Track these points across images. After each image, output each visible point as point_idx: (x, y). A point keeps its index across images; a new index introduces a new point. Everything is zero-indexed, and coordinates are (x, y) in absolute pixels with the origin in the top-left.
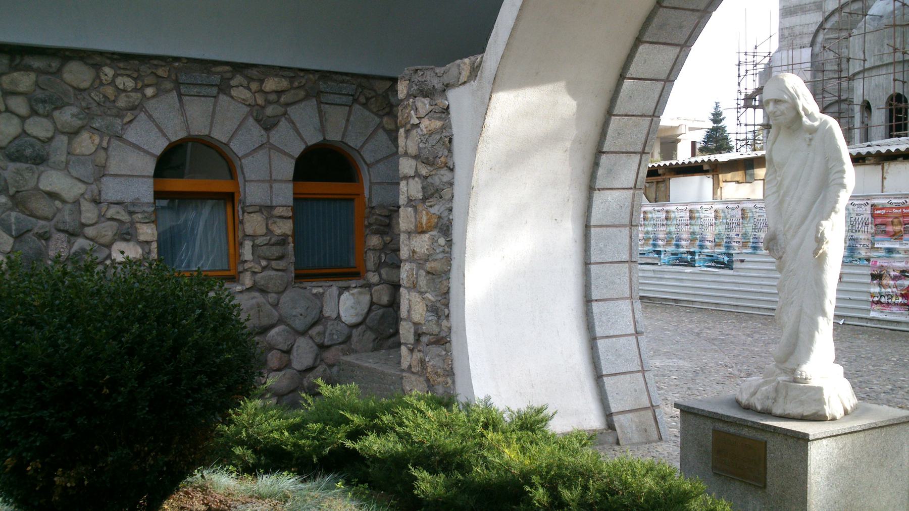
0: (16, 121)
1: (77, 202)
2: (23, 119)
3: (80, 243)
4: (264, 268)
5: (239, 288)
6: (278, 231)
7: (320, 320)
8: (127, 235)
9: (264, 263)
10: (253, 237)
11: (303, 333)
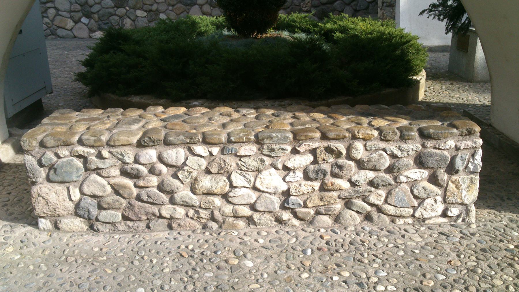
11: (349, 4)
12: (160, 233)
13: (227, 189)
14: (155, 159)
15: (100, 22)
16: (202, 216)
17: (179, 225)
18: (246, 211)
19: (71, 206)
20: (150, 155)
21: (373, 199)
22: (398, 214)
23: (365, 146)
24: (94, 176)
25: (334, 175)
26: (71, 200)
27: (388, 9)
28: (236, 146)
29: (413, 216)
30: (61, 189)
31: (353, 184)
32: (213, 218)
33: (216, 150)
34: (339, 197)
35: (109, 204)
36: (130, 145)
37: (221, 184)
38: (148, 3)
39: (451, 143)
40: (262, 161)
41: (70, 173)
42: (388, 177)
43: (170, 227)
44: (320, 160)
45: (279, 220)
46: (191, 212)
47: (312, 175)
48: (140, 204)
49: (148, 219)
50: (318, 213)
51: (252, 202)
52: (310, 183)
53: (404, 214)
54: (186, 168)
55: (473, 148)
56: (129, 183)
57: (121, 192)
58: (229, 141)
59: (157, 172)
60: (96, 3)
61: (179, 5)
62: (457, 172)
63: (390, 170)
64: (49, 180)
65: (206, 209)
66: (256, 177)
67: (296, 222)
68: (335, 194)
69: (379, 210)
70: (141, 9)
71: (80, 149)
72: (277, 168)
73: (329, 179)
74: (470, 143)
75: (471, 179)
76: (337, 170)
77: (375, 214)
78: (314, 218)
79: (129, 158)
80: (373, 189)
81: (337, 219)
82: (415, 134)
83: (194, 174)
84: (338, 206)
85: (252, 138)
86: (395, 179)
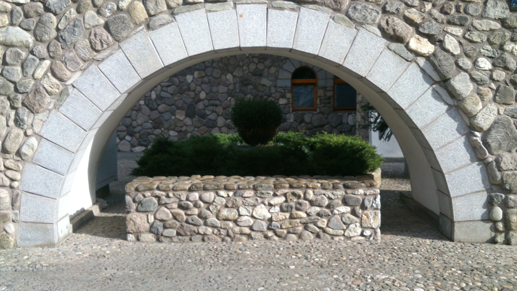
0: (255, 65)
1: (270, 87)
2: (257, 64)
4: (323, 107)
5: (315, 113)
6: (328, 95)
7: (341, 123)
8: (283, 96)
9: (323, 105)
10: (320, 97)
11: (335, 128)
12: (197, 242)
13: (237, 216)
14: (198, 198)
15: (140, 140)
16: (222, 233)
17: (208, 238)
18: (247, 231)
19: (147, 226)
20: (195, 195)
21: (320, 224)
22: (335, 233)
23: (314, 192)
24: (163, 208)
25: (298, 209)
26: (148, 222)
27: (363, 130)
28: (242, 191)
29: (344, 235)
30: (144, 216)
31: (308, 215)
32: (228, 235)
33: (231, 194)
34: (301, 223)
35: (170, 225)
36: (185, 190)
37: (233, 213)
38: (179, 125)
39: (361, 191)
40: (257, 200)
41: (149, 206)
42: (328, 211)
43: (203, 240)
44: (289, 200)
45: (266, 237)
46: (216, 231)
47: (285, 209)
48: (188, 225)
49: (191, 235)
50: (289, 232)
51: (251, 224)
52: (284, 214)
53: (338, 233)
54: (214, 204)
55: (374, 194)
56: (182, 212)
57: (177, 217)
58: (239, 188)
59: (198, 206)
60: (138, 125)
61: (203, 127)
62: (366, 208)
63: (328, 207)
64: (137, 210)
65: (224, 229)
66: (253, 210)
67: (276, 238)
68: (298, 221)
69: (324, 231)
70: (173, 130)
71: (158, 192)
72: (265, 205)
73: (294, 212)
74: (372, 192)
75: (375, 213)
76: (298, 206)
77: (321, 234)
78: (286, 236)
79: (183, 198)
80: (319, 218)
81: (300, 236)
82: (341, 186)
83: (219, 207)
84: (300, 228)
85: (251, 186)
86: (332, 212)
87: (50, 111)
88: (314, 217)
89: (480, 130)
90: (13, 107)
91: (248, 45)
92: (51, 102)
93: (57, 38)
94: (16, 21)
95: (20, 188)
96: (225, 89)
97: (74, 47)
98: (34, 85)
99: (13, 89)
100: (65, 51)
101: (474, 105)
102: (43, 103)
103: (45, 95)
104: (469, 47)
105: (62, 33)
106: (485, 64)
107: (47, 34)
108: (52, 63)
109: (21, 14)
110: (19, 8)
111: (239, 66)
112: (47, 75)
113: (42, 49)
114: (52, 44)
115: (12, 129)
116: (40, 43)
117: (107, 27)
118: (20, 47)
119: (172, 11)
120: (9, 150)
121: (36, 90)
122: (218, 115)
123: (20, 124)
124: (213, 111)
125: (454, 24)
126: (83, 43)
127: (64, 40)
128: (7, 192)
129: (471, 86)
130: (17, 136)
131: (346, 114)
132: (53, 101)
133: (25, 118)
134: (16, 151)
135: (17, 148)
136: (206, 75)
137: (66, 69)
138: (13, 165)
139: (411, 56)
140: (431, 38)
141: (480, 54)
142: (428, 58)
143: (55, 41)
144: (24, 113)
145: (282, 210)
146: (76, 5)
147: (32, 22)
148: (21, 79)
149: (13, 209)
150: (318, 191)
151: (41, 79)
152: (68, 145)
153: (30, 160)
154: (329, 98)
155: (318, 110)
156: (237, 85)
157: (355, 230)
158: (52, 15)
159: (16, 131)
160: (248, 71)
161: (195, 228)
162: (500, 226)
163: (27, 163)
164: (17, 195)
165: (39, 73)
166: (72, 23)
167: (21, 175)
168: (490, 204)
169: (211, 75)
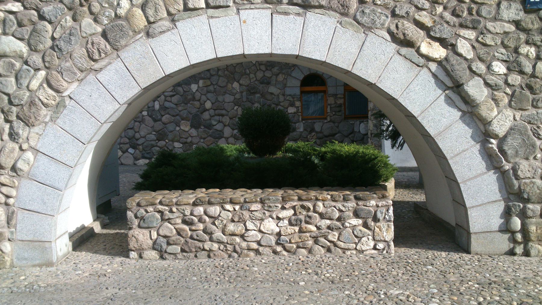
0: (262, 72)
1: (278, 95)
2: (264, 72)
3: (279, 107)
4: (334, 115)
5: (326, 121)
6: (338, 103)
7: (353, 132)
8: (292, 105)
9: (334, 113)
10: (330, 105)
11: (347, 136)
12: (203, 259)
13: (244, 231)
14: (202, 213)
15: (144, 152)
16: (229, 249)
17: (215, 255)
18: (255, 246)
19: (150, 242)
20: (200, 210)
21: (330, 237)
22: (346, 247)
23: (323, 204)
24: (167, 224)
25: (307, 223)
26: (151, 239)
27: (375, 138)
28: (249, 205)
29: (356, 249)
30: (146, 232)
31: (318, 228)
32: (235, 251)
33: (237, 207)
34: (310, 236)
35: (174, 241)
36: (189, 204)
37: (240, 228)
38: (184, 136)
39: (373, 203)
40: (264, 213)
41: (152, 222)
42: (338, 224)
43: (209, 256)
44: (298, 212)
45: (275, 252)
46: (222, 247)
47: (294, 223)
48: (192, 241)
49: (196, 251)
50: (298, 247)
51: (259, 239)
52: (293, 227)
53: (350, 247)
54: (220, 218)
55: (386, 206)
56: (187, 228)
57: (181, 233)
58: (245, 202)
59: (203, 221)
60: (141, 137)
61: (209, 138)
62: (379, 220)
63: (339, 219)
64: (139, 226)
65: (231, 244)
66: (261, 224)
67: (285, 253)
68: (308, 234)
69: (335, 245)
70: (178, 141)
71: (160, 207)
72: (273, 218)
73: (304, 225)
74: (384, 203)
75: (388, 225)
76: (308, 219)
77: (332, 248)
78: (296, 250)
79: (188, 212)
80: (330, 231)
81: (310, 251)
82: (352, 197)
83: (225, 222)
84: (310, 242)
85: (258, 200)
86: (343, 225)
87: (46, 123)
88: (324, 230)
89: (496, 137)
90: (7, 121)
91: (253, 52)
92: (47, 115)
93: (52, 48)
94: (9, 30)
95: (16, 205)
96: (232, 98)
97: (70, 57)
98: (28, 97)
99: (7, 101)
100: (60, 60)
101: (489, 111)
102: (39, 115)
103: (41, 107)
104: (482, 51)
105: (58, 43)
106: (500, 68)
107: (42, 43)
108: (47, 74)
109: (14, 23)
110: (11, 17)
111: (245, 74)
112: (43, 86)
113: (36, 59)
114: (47, 54)
115: (7, 143)
116: (34, 53)
117: (104, 35)
118: (13, 57)
119: (172, 18)
120: (3, 165)
121: (31, 102)
122: (225, 126)
123: (15, 138)
124: (219, 122)
125: (467, 27)
126: (79, 52)
127: (60, 50)
128: (2, 209)
129: (486, 91)
130: (12, 151)
131: (358, 122)
132: (50, 113)
133: (21, 132)
134: (11, 166)
135: (12, 163)
136: (212, 84)
137: (62, 79)
138: (8, 181)
139: (422, 61)
140: (442, 42)
141: (494, 58)
142: (440, 63)
143: (50, 50)
144: (19, 126)
145: (291, 224)
146: (72, 13)
147: (26, 31)
148: (15, 91)
149: (9, 227)
150: (328, 203)
151: (36, 90)
152: (66, 159)
153: (26, 175)
154: (340, 106)
155: (329, 119)
156: (244, 94)
157: (367, 244)
158: (46, 23)
159: (11, 145)
160: (255, 79)
161: (200, 245)
162: (519, 237)
163: (22, 179)
164: (13, 213)
165: (35, 84)
166: (68, 32)
167: (17, 192)
168: (507, 214)
169: (217, 84)
